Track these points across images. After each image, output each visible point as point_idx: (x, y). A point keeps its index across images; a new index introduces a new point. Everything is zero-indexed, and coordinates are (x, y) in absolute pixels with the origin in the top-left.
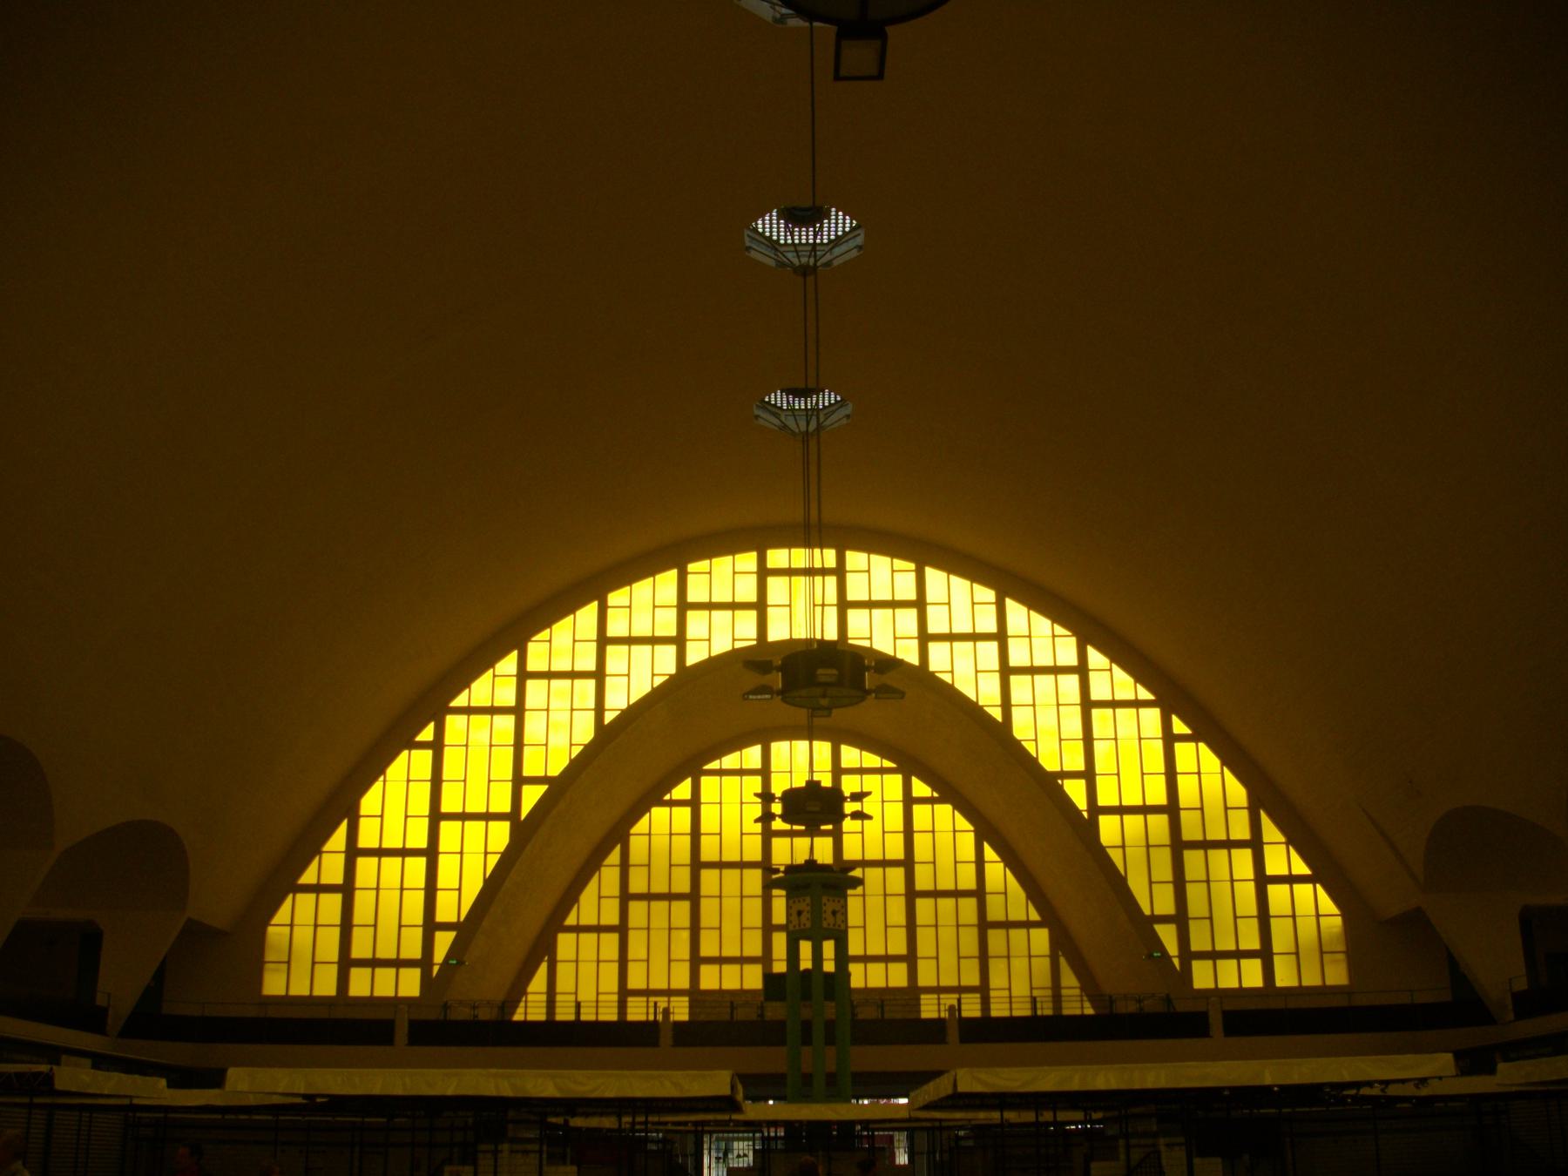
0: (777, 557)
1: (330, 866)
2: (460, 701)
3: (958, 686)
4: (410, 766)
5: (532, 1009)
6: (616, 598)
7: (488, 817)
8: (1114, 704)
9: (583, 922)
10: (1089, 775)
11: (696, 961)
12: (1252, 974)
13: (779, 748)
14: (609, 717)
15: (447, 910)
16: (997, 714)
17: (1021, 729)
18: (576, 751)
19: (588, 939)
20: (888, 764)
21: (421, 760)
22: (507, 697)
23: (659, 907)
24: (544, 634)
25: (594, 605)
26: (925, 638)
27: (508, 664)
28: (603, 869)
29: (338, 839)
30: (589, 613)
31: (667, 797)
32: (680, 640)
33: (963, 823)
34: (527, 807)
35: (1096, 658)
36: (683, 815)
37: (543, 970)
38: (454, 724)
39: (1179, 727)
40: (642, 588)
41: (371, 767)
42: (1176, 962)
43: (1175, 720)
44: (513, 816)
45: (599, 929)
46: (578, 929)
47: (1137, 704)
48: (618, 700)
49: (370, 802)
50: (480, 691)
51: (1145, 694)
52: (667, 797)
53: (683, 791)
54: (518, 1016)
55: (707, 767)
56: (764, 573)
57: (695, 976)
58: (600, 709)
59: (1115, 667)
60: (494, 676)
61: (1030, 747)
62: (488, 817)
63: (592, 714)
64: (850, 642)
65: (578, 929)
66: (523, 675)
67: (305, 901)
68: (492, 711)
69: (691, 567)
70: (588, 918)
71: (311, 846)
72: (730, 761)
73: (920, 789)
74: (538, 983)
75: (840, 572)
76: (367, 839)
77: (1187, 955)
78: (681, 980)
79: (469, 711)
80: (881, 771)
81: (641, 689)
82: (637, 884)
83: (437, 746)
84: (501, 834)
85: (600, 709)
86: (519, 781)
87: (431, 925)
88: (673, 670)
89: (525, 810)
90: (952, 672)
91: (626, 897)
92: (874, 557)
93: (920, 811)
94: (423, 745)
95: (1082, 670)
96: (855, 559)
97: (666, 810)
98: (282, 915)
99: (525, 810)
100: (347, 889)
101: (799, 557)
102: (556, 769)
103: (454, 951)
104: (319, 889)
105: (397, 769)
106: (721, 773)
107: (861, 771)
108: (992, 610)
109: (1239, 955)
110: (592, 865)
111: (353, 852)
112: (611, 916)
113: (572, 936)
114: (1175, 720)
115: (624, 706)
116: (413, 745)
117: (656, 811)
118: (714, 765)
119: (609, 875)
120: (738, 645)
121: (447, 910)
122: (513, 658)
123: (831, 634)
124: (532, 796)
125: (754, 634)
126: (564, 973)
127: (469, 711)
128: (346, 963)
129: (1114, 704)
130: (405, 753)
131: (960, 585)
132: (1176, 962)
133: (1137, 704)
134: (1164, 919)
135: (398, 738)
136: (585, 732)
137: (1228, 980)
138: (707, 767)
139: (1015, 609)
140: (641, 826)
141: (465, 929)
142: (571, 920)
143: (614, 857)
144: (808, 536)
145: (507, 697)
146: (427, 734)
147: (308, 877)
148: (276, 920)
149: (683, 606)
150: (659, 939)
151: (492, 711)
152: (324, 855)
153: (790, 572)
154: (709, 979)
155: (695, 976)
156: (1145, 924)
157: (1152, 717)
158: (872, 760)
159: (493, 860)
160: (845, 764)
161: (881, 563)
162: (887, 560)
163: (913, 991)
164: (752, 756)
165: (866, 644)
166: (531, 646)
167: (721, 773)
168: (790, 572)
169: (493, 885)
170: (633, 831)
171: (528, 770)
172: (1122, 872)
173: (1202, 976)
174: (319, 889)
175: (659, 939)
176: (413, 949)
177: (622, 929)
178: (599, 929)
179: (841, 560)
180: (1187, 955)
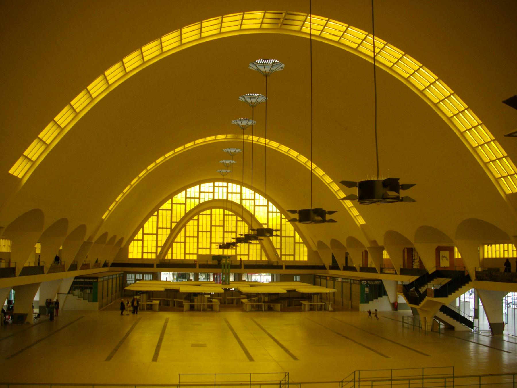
0: (216, 184)
1: (139, 236)
2: (161, 208)
3: (246, 208)
4: (153, 219)
5: (168, 257)
6: (188, 190)
7: (166, 228)
8: (273, 212)
9: (178, 241)
10: (267, 224)
11: (198, 248)
12: (292, 258)
13: (214, 210)
14: (187, 211)
15: (160, 244)
16: (253, 213)
17: (257, 216)
18: (181, 217)
19: (179, 244)
20: (233, 214)
21: (155, 218)
22: (169, 208)
23: (192, 238)
24: (176, 196)
25: (184, 192)
26: (241, 199)
27: (169, 201)
28: (181, 232)
29: (141, 232)
30: (184, 192)
31: (193, 219)
32: (199, 198)
33: (246, 225)
34: (173, 227)
35: (270, 204)
36: (196, 222)
37: (171, 249)
38: (160, 212)
39: (283, 216)
40: (193, 188)
41: (146, 219)
42: (279, 256)
43: (283, 215)
44: (171, 228)
45: (181, 242)
46: (177, 242)
47: (276, 212)
48: (188, 209)
49: (146, 225)
50: (164, 206)
51: (278, 211)
52: (193, 219)
53: (196, 218)
54: (166, 258)
55: (201, 213)
56: (214, 186)
57: (198, 251)
58: (185, 210)
59: (274, 206)
60: (167, 204)
61: (258, 219)
62: (166, 228)
63: (184, 211)
64: (229, 200)
65: (177, 242)
66: (172, 204)
67: (135, 242)
68: (167, 210)
69: (202, 185)
70: (179, 241)
71: (136, 233)
72: (205, 212)
73: (239, 218)
74: (170, 252)
75: (227, 187)
76: (145, 232)
77: (281, 255)
78: (195, 252)
79: (163, 210)
80: (231, 215)
81: (192, 207)
82: (188, 235)
83: (157, 216)
84: (169, 232)
85: (185, 210)
86: (172, 222)
87: (157, 247)
88: (198, 204)
89: (173, 227)
90: (246, 206)
91: (185, 237)
92: (233, 184)
93: (239, 223)
94: (155, 216)
95: (268, 206)
96: (230, 184)
97: (193, 221)
98: (131, 244)
99: (173, 227)
100: (142, 240)
101: (221, 184)
102: (178, 220)
103: (161, 251)
104: (138, 240)
105: (151, 219)
106: (203, 214)
107: (228, 215)
108: (253, 195)
109: (290, 255)
110: (180, 231)
111: (143, 234)
112: (183, 240)
113: (176, 244)
114: (283, 215)
115: (190, 210)
116: (153, 215)
117: (191, 221)
118: (202, 213)
119: (183, 232)
120: (210, 199)
121: (160, 244)
122: (170, 200)
123: (225, 198)
124: (174, 225)
125: (212, 198)
126: (174, 250)
127: (163, 210)
128: (143, 253)
129: (273, 212)
130: (152, 217)
131: (248, 190)
132: (279, 256)
133: (276, 212)
134: (278, 249)
135: (151, 214)
136: (183, 214)
137: (288, 259)
138: (201, 213)
139: (257, 195)
140: (188, 224)
141: (163, 247)
142: (176, 241)
143: (183, 229)
144: (223, 180)
145: (169, 208)
146: (156, 214)
147: (136, 238)
148: (130, 245)
149: (200, 192)
150: (191, 244)
151: (167, 210)
152: (138, 234)
153: (219, 187)
154: (201, 252)
155: (198, 251)
156: (274, 250)
157: (279, 215)
158: (230, 213)
159: (167, 236)
160: (225, 214)
161: (234, 185)
162: (235, 185)
163: (236, 255)
164: (209, 211)
165: (231, 200)
166: (173, 198)
167: (203, 214)
168: (219, 187)
169: (167, 240)
170: (187, 225)
171: (173, 221)
172: (272, 240)
173: (284, 258)
174: (138, 240)
175: (191, 244)
176: (154, 251)
177: (185, 242)
178: (181, 242)
179: (227, 185)
180: (281, 255)
